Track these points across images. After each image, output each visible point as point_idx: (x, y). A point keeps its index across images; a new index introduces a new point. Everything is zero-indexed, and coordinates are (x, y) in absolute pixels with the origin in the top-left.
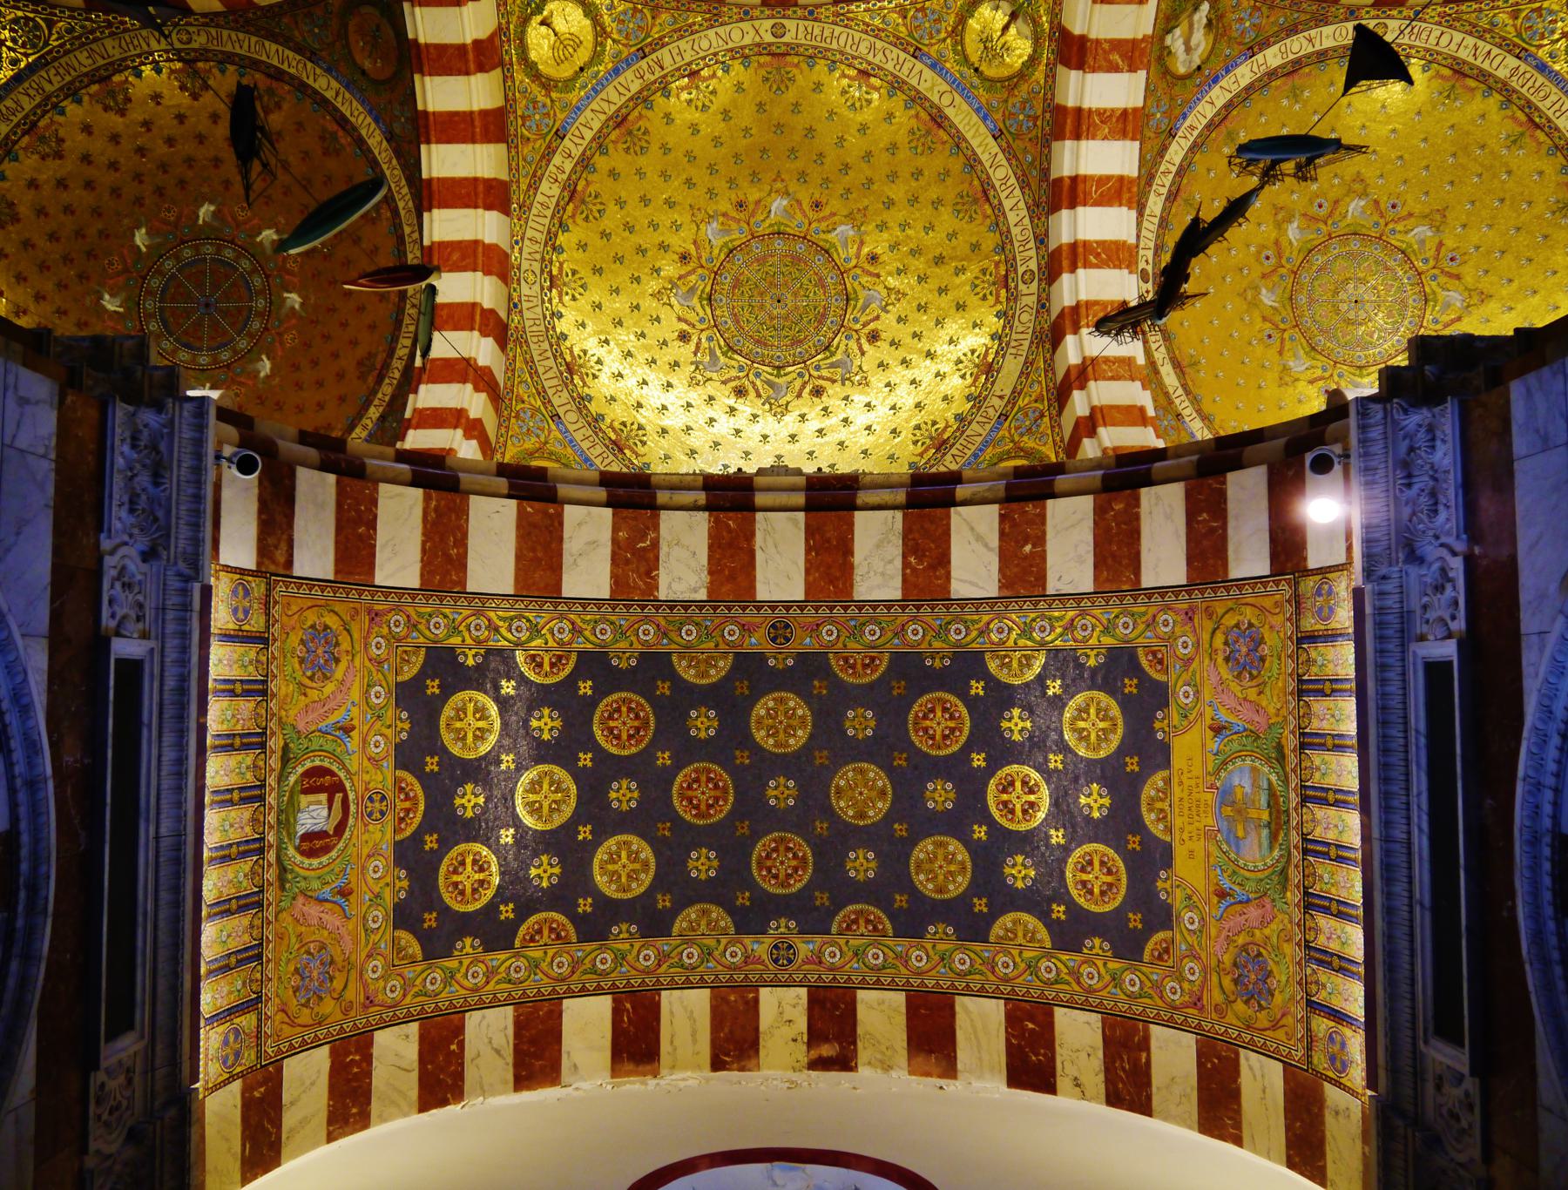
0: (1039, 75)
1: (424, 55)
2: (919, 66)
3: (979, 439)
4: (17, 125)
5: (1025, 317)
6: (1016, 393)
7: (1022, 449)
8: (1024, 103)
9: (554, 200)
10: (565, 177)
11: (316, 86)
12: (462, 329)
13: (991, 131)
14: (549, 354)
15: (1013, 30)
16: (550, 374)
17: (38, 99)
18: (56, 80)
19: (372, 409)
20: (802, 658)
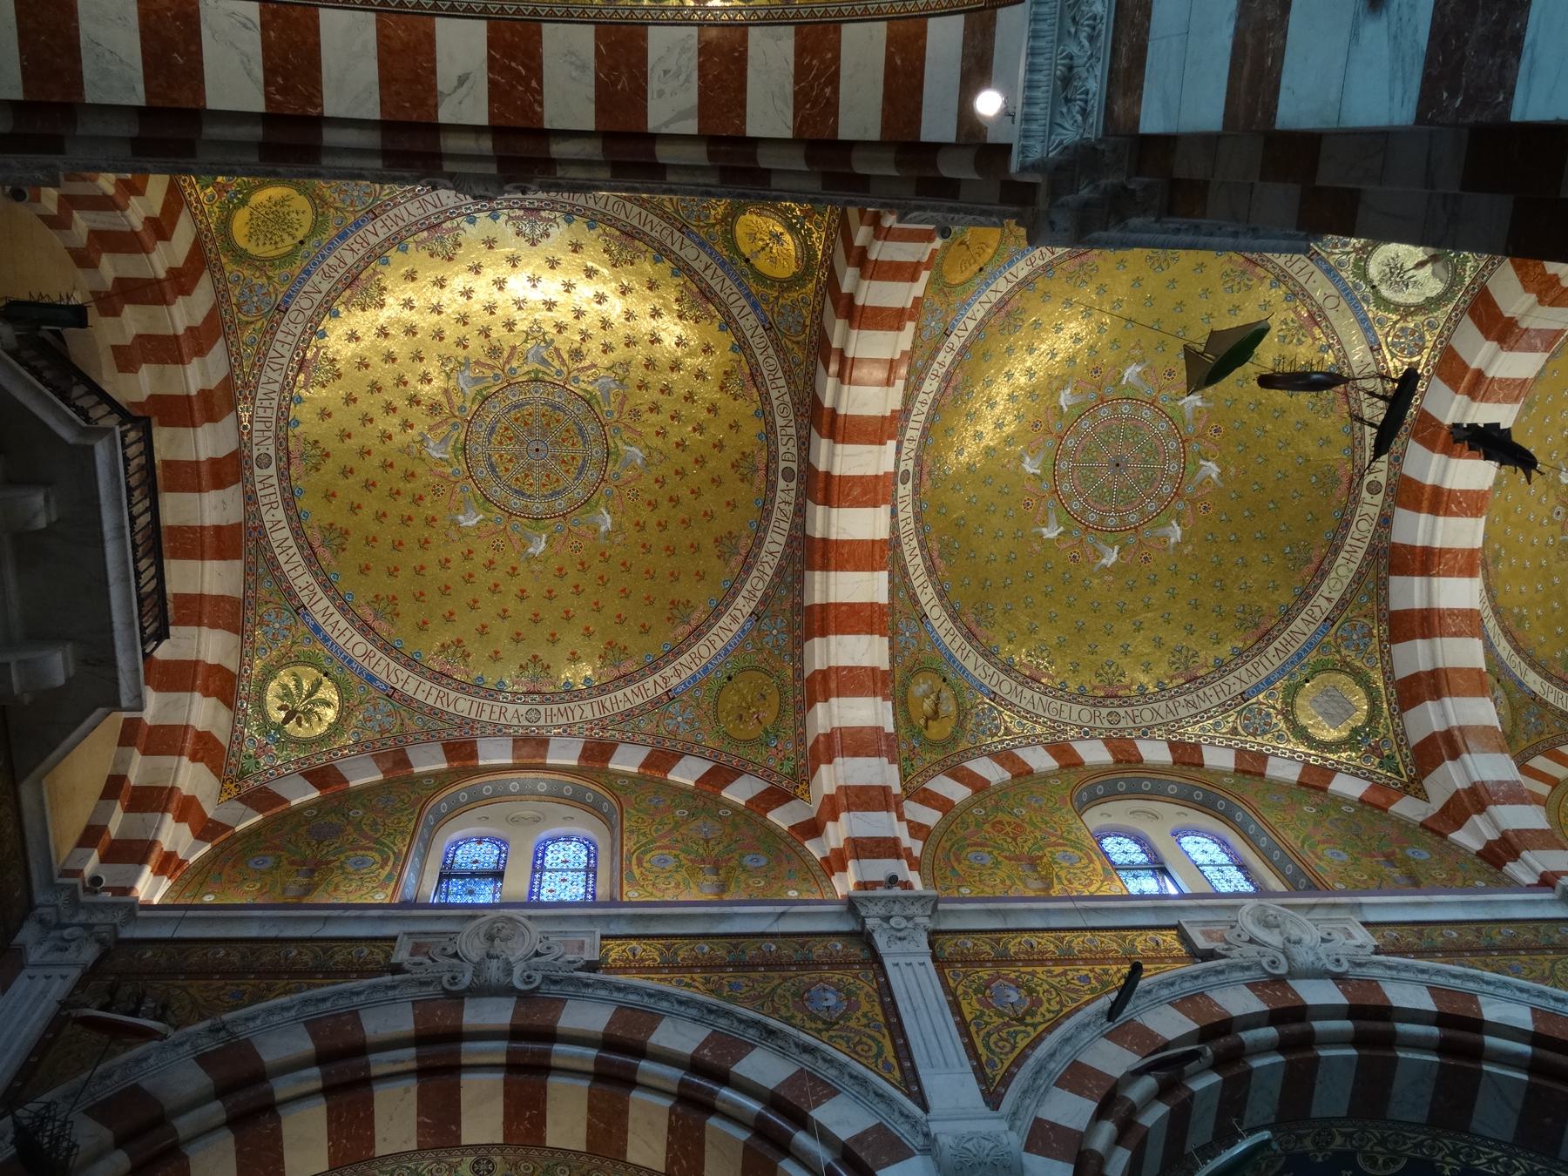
0: (1441, 315)
1: (857, 315)
2: (1312, 267)
3: (1304, 639)
4: (339, 281)
5: (1363, 526)
6: (1343, 604)
7: (1348, 664)
8: (1413, 332)
9: (932, 395)
10: (944, 370)
11: (682, 254)
12: (863, 570)
13: (1369, 342)
14: (917, 551)
15: (1428, 269)
16: (919, 572)
17: (362, 252)
18: (380, 231)
19: (740, 601)
20: (1335, 1153)
